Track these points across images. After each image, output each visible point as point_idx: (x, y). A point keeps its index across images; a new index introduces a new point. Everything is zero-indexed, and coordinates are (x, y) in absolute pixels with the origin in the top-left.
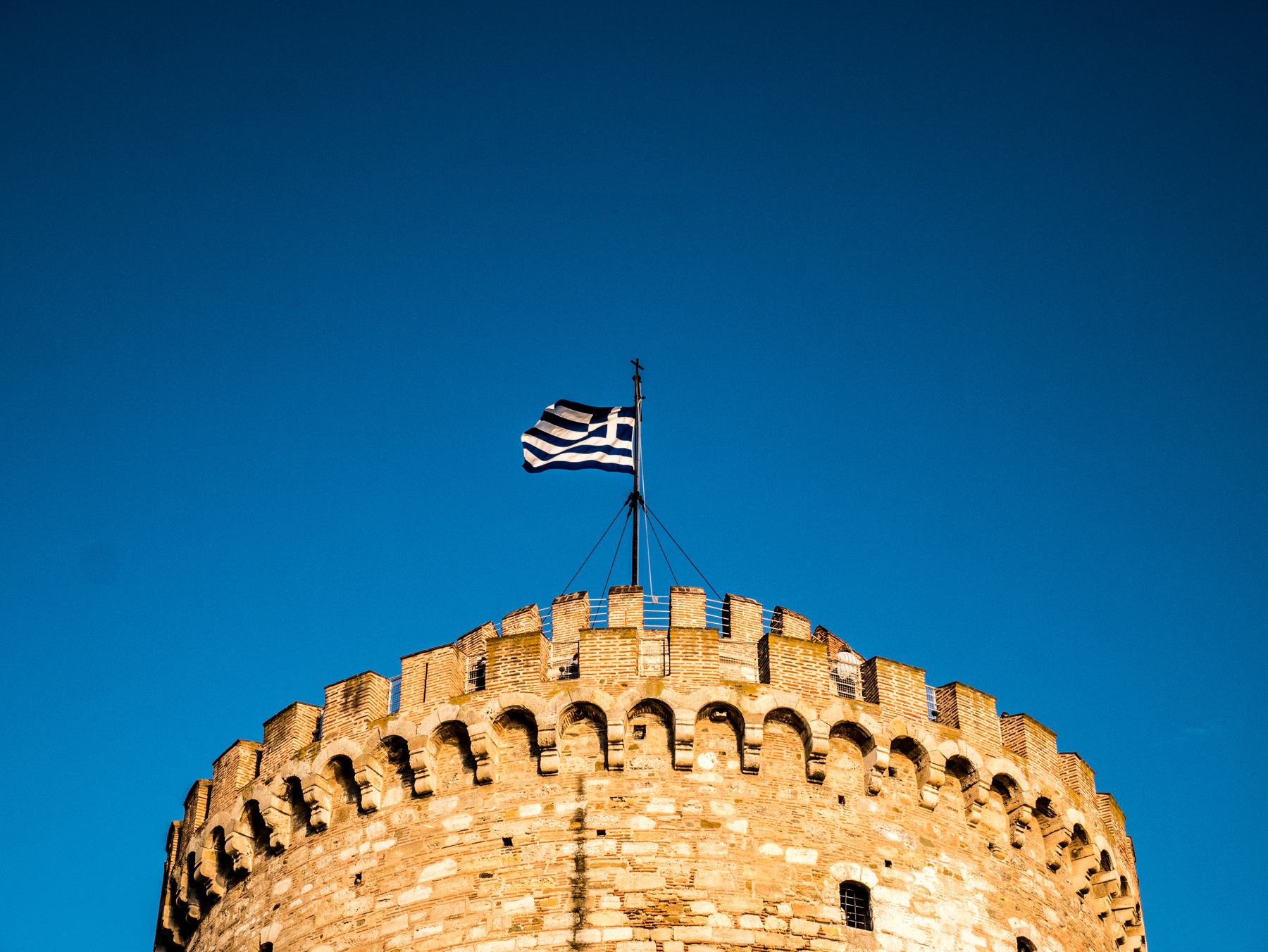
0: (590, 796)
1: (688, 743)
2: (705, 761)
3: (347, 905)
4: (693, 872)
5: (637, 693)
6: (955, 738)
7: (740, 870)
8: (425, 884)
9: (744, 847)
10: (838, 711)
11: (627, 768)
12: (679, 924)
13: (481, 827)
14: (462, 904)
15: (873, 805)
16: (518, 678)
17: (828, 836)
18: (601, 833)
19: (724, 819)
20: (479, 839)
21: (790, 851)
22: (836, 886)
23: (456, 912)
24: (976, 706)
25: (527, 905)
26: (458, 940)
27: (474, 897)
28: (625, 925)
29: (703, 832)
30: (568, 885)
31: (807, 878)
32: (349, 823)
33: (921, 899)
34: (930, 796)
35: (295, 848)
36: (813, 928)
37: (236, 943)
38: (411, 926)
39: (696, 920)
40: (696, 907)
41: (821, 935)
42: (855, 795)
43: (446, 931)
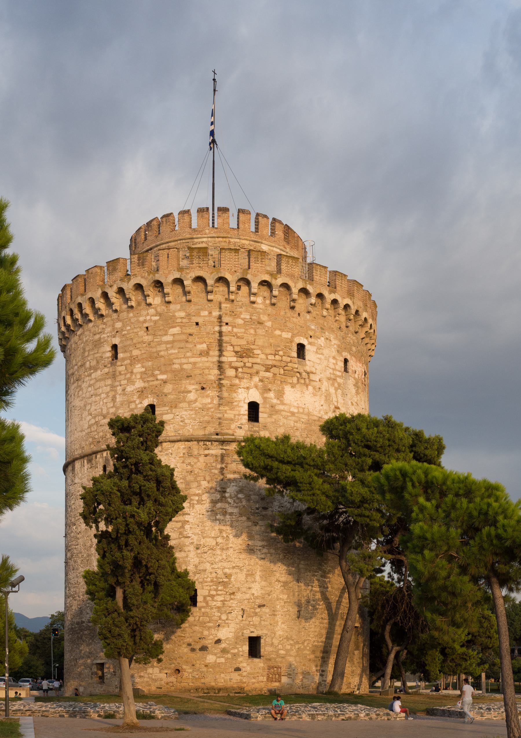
0: (223, 310)
1: (255, 294)
2: (259, 300)
3: (144, 337)
4: (255, 339)
5: (239, 275)
6: (334, 292)
7: (269, 340)
8: (171, 335)
9: (270, 331)
10: (300, 285)
11: (235, 301)
12: (251, 357)
13: (189, 317)
14: (183, 344)
15: (308, 316)
16: (200, 265)
17: (294, 328)
18: (227, 324)
19: (264, 321)
20: (188, 321)
21: (284, 333)
22: (296, 345)
23: (182, 346)
24: (341, 279)
25: (204, 346)
26: (183, 356)
27: (187, 342)
28: (235, 356)
29: (258, 326)
30: (217, 341)
31: (288, 343)
32: (142, 307)
33: (319, 348)
34: (325, 313)
35: (122, 312)
36: (289, 359)
37: (102, 341)
38: (167, 349)
39: (255, 356)
40: (256, 352)
41: (291, 362)
42: (303, 313)
43: (179, 352)
